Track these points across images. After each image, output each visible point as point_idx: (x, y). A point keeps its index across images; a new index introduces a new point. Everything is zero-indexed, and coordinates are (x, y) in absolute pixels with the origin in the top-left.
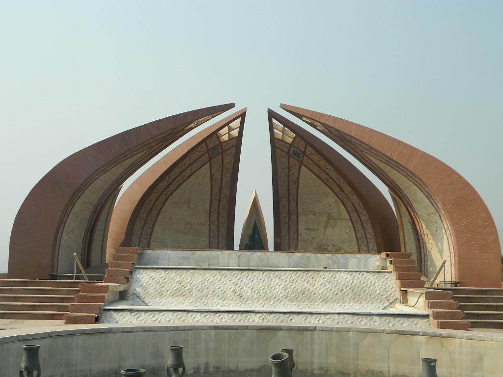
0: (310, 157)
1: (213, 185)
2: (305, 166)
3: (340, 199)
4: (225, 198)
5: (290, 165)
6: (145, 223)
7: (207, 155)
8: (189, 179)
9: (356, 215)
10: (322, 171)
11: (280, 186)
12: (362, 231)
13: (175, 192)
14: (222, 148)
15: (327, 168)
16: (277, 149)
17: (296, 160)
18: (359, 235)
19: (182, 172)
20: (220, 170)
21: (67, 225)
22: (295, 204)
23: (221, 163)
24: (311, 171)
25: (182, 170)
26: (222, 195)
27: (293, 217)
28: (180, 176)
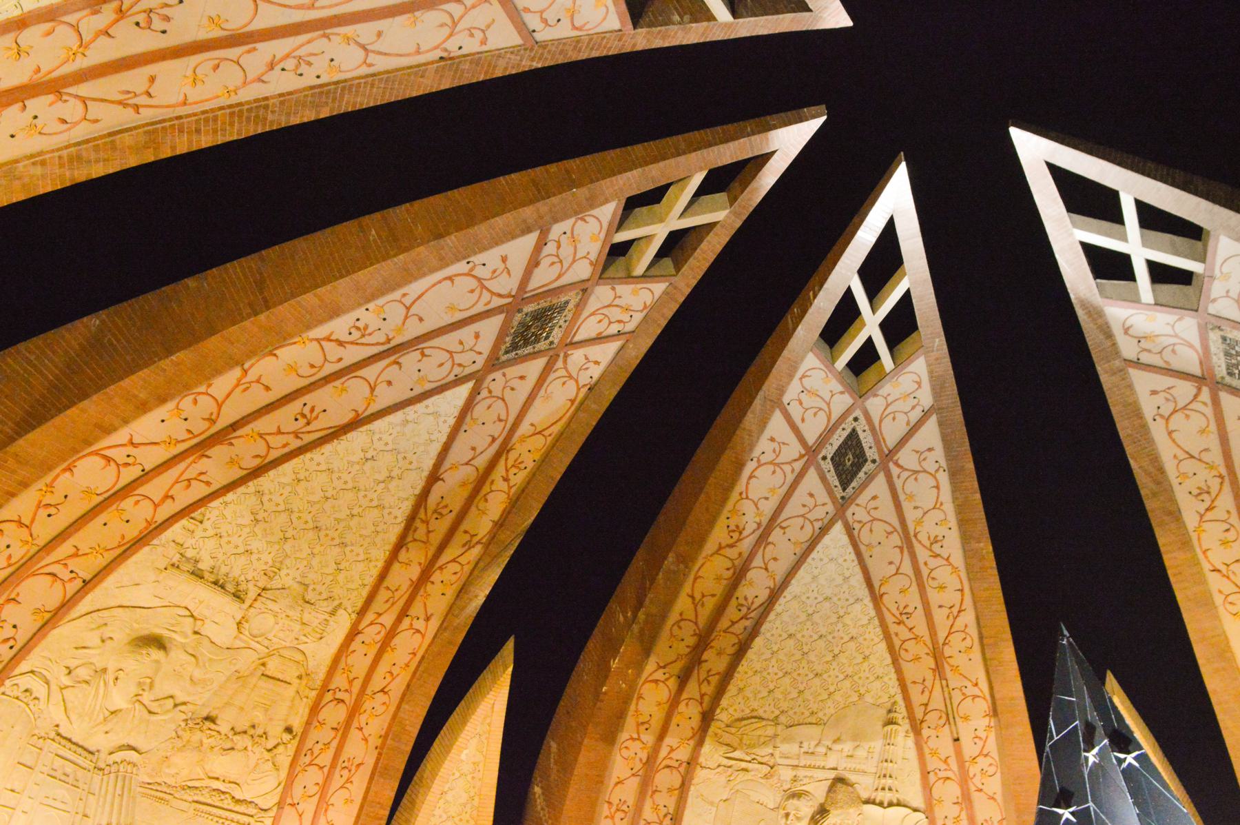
0: (898, 484)
1: (410, 538)
2: (849, 530)
3: (911, 717)
4: (418, 631)
5: (783, 516)
7: (490, 328)
8: (327, 448)
9: (958, 792)
10: (907, 567)
11: (673, 617)
13: (215, 504)
14: (580, 306)
15: (936, 556)
16: (777, 420)
17: (830, 493)
19: (327, 380)
22: (696, 721)
24: (859, 554)
25: (329, 369)
27: (666, 779)
28: (295, 407)
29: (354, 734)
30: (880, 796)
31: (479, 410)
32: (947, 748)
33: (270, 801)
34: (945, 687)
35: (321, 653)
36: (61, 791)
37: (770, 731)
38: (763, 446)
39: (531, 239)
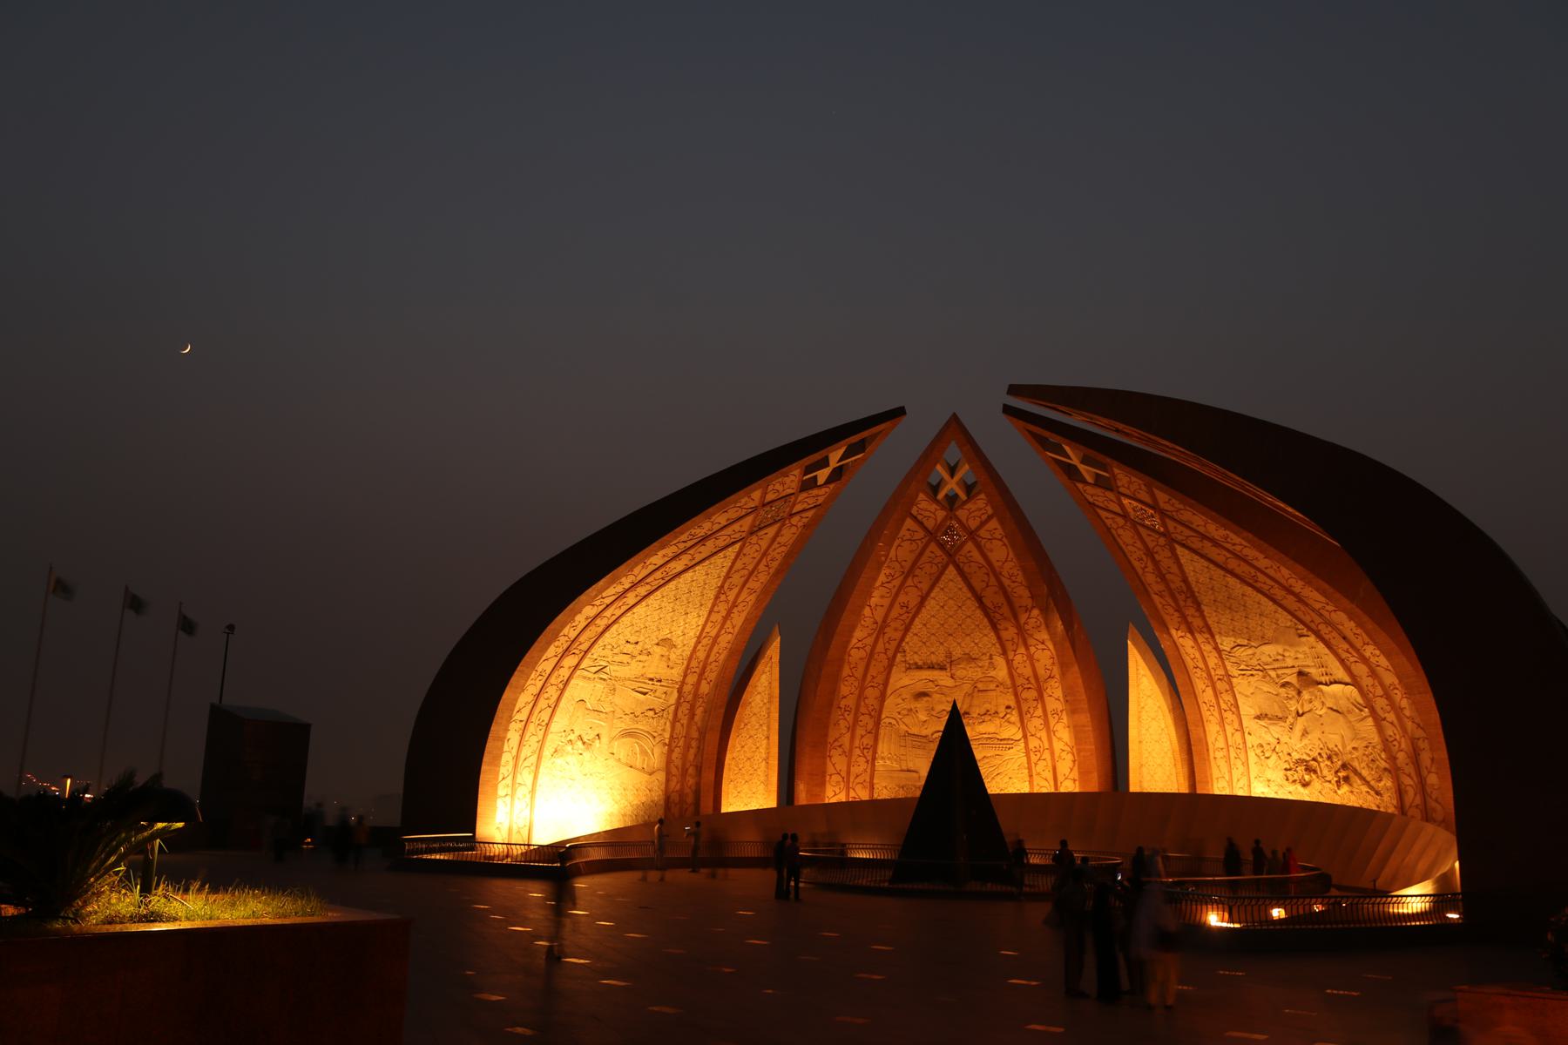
2: (1183, 545)
3: (1309, 629)
6: (856, 721)
12: (1391, 717)
14: (959, 522)
18: (1390, 731)
19: (897, 594)
20: (993, 581)
21: (554, 727)
23: (981, 560)
24: (1202, 556)
26: (1031, 641)
28: (897, 606)
29: (1047, 699)
30: (1323, 679)
31: (966, 569)
32: (1346, 646)
33: (1019, 735)
34: (1313, 610)
35: (1002, 673)
36: (920, 752)
37: (1250, 651)
38: (1108, 522)
39: (909, 523)
